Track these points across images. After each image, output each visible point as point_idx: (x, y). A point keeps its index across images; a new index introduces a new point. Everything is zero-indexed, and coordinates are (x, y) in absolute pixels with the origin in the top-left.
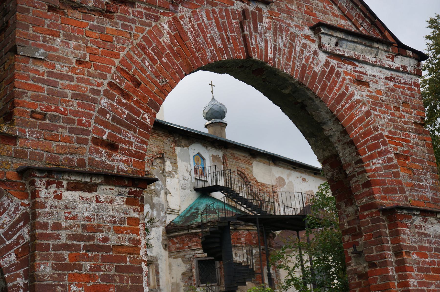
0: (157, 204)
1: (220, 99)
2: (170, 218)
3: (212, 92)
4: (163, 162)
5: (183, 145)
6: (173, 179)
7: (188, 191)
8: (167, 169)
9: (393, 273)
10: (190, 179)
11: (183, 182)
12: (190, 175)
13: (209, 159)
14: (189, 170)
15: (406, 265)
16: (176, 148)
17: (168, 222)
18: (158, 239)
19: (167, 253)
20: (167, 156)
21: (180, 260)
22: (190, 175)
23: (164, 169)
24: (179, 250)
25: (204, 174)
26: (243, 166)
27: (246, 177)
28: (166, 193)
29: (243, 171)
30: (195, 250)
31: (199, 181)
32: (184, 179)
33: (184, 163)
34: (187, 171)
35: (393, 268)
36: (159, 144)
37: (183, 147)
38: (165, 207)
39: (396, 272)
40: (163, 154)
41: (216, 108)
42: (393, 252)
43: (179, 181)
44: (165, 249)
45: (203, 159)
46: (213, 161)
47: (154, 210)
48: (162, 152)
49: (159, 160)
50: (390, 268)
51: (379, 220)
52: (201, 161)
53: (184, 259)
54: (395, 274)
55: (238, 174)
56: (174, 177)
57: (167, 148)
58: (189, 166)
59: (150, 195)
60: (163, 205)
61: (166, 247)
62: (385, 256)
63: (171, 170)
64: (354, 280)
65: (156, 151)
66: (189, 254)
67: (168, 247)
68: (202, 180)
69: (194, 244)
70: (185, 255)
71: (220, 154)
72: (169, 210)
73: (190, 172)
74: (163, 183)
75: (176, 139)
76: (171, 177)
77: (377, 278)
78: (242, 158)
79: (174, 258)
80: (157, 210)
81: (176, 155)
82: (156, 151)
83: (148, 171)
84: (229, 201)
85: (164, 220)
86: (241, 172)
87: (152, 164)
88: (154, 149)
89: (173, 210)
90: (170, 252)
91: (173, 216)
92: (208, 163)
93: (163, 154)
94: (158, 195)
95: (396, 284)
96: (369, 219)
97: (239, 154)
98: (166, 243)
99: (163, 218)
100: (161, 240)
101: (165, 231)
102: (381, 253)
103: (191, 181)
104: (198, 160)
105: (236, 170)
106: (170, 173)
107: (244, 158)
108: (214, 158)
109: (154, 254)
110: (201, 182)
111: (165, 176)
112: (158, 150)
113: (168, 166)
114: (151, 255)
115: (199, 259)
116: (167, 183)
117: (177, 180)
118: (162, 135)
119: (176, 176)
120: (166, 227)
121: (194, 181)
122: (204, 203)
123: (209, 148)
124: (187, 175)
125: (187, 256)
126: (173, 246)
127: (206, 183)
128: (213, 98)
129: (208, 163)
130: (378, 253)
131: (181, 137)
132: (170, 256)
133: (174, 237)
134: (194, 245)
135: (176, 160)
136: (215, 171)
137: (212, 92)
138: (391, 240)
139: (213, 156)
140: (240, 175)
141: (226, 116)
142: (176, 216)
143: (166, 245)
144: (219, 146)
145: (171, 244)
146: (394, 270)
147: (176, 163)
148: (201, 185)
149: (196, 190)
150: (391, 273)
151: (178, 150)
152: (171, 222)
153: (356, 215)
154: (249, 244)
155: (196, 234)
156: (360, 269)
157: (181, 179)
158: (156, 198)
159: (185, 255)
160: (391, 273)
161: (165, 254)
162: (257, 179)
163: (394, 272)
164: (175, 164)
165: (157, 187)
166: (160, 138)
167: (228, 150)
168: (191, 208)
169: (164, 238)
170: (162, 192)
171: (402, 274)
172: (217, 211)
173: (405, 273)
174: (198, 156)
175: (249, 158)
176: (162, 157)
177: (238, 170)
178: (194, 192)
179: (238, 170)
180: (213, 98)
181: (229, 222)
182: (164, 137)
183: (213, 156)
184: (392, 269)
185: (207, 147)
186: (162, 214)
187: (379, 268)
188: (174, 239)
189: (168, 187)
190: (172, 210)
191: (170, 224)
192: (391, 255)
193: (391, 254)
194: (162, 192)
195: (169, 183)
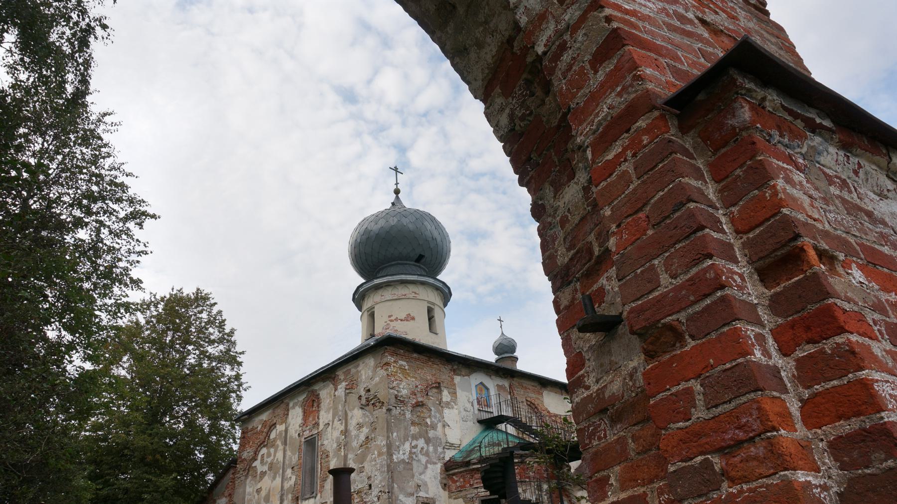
0: (434, 438)
1: (509, 334)
2: (449, 454)
3: (501, 327)
4: (440, 392)
5: (463, 374)
6: (451, 410)
7: (470, 424)
8: (444, 399)
9: (766, 353)
10: (472, 410)
11: (464, 413)
12: (472, 405)
13: (493, 389)
14: (471, 400)
15: (831, 301)
16: (455, 377)
17: (447, 459)
18: (435, 478)
19: (447, 493)
20: (445, 385)
21: (461, 500)
22: (472, 405)
23: (441, 399)
24: (461, 489)
25: (488, 406)
26: (532, 396)
27: (536, 407)
28: (444, 426)
29: (533, 401)
30: (477, 488)
31: (482, 412)
32: (465, 410)
33: (465, 393)
34: (469, 402)
35: (766, 332)
36: (434, 372)
37: (464, 376)
38: (444, 441)
39: (785, 352)
40: (439, 383)
41: (505, 342)
42: (751, 262)
43: (460, 412)
44: (444, 489)
45: (487, 389)
46: (498, 390)
47: (430, 445)
48: (438, 381)
49: (435, 390)
50: (751, 331)
51: (668, 149)
52: (484, 392)
53: (466, 499)
54: (777, 360)
55: (527, 404)
56: (453, 408)
57: (444, 377)
58: (470, 396)
59: (424, 429)
60: (440, 439)
61: (445, 486)
62: (718, 276)
63: (449, 400)
64: (600, 439)
65: (431, 379)
66: (472, 493)
67: (447, 486)
68: (486, 411)
69: (476, 481)
70: (466, 495)
71: (506, 383)
72: (448, 444)
73: (472, 403)
74: (440, 414)
75: (455, 367)
76: (449, 408)
77: (689, 391)
78: (531, 387)
79: (455, 499)
80: (433, 445)
81: (455, 385)
82: (431, 379)
83: (421, 402)
84: (518, 433)
85: (442, 456)
86: (531, 403)
87: (427, 394)
88: (428, 378)
89: (453, 444)
90: (450, 492)
91: (453, 451)
92: (493, 392)
93: (439, 383)
94: (434, 427)
95: (794, 408)
96: (627, 167)
97: (526, 383)
98: (445, 481)
99: (441, 453)
100: (439, 478)
101: (444, 469)
102: (694, 271)
103: (474, 412)
104: (481, 390)
105: (524, 400)
106: (448, 404)
107: (533, 388)
108: (500, 387)
109: (431, 495)
110: (484, 413)
111: (442, 407)
112: (434, 379)
113: (446, 396)
114: (427, 496)
115: (482, 498)
116: (444, 414)
117: (456, 411)
118: (439, 363)
119: (456, 407)
120: (445, 464)
121: (476, 412)
122: (493, 436)
123: (493, 377)
124: (469, 406)
125: (469, 496)
126: (453, 485)
127: (489, 414)
128: (503, 333)
129: (493, 392)
130: (679, 281)
131: (461, 365)
132: (450, 497)
133: (454, 474)
134: (477, 483)
135: (455, 389)
136: (498, 402)
137: (501, 327)
138: (732, 221)
139: (498, 385)
140: (529, 405)
141: (517, 350)
142: (456, 451)
143: (445, 485)
144: (504, 374)
145: (451, 483)
146: (770, 341)
147: (456, 393)
148: (486, 416)
149: (480, 422)
150: (758, 354)
151: (457, 379)
152: (451, 458)
153: (587, 199)
154: (539, 481)
155: (477, 469)
156: (616, 387)
157: (462, 410)
158: (432, 431)
159: (466, 495)
160: (758, 354)
161: (444, 494)
162: (549, 409)
163: (774, 353)
164: (454, 394)
165: (433, 419)
166: (435, 366)
167: (515, 379)
168: (474, 442)
169: (442, 476)
170: (440, 425)
171: (822, 352)
172: (502, 443)
173: (839, 339)
174: (481, 386)
175: (539, 387)
176: (438, 387)
177: (527, 400)
178: (478, 424)
179: (527, 400)
180: (503, 333)
181: (512, 453)
182: (440, 365)
183: (498, 385)
184: (760, 338)
185: (490, 376)
186: (440, 449)
187: (691, 343)
188: (454, 477)
189: (445, 419)
190: (452, 445)
191: (449, 460)
192: (743, 279)
193: (741, 276)
194: (440, 425)
195: (447, 414)
